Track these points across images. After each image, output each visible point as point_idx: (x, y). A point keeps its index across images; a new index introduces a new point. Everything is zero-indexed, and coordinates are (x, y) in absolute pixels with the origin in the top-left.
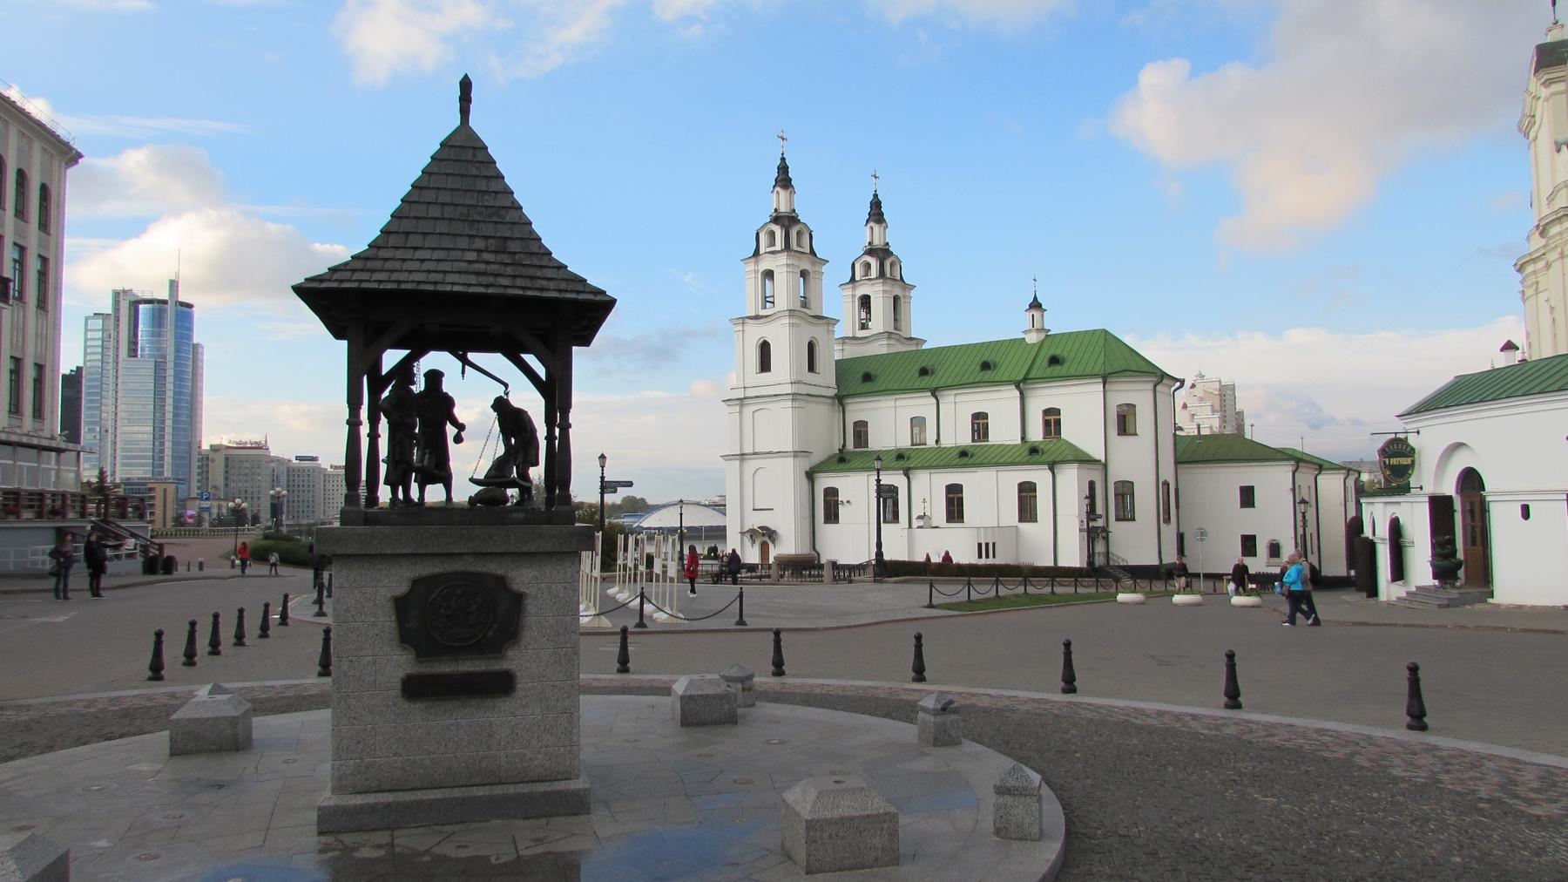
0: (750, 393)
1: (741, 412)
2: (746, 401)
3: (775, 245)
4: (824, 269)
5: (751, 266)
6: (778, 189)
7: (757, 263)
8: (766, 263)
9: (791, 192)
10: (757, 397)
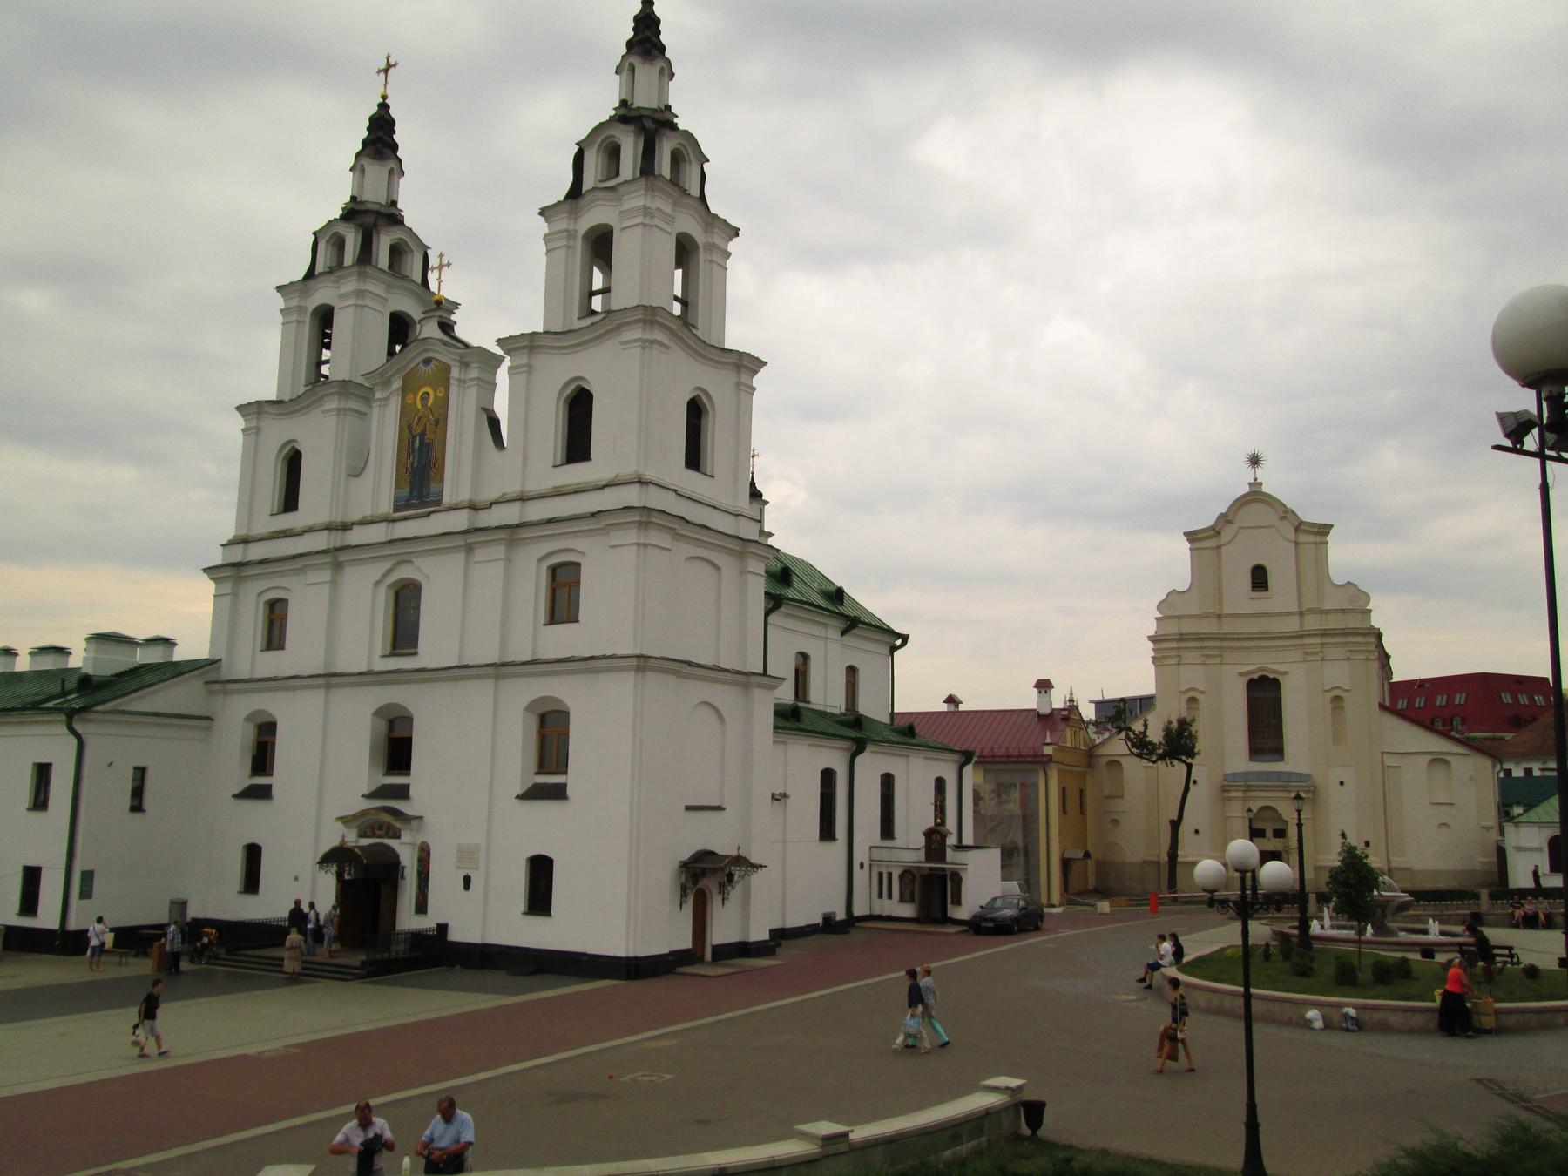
0: (537, 511)
1: (508, 560)
2: (525, 534)
3: (617, 174)
4: (733, 246)
5: (562, 225)
6: (635, 60)
7: (575, 214)
8: (596, 215)
9: (661, 72)
10: (549, 521)
